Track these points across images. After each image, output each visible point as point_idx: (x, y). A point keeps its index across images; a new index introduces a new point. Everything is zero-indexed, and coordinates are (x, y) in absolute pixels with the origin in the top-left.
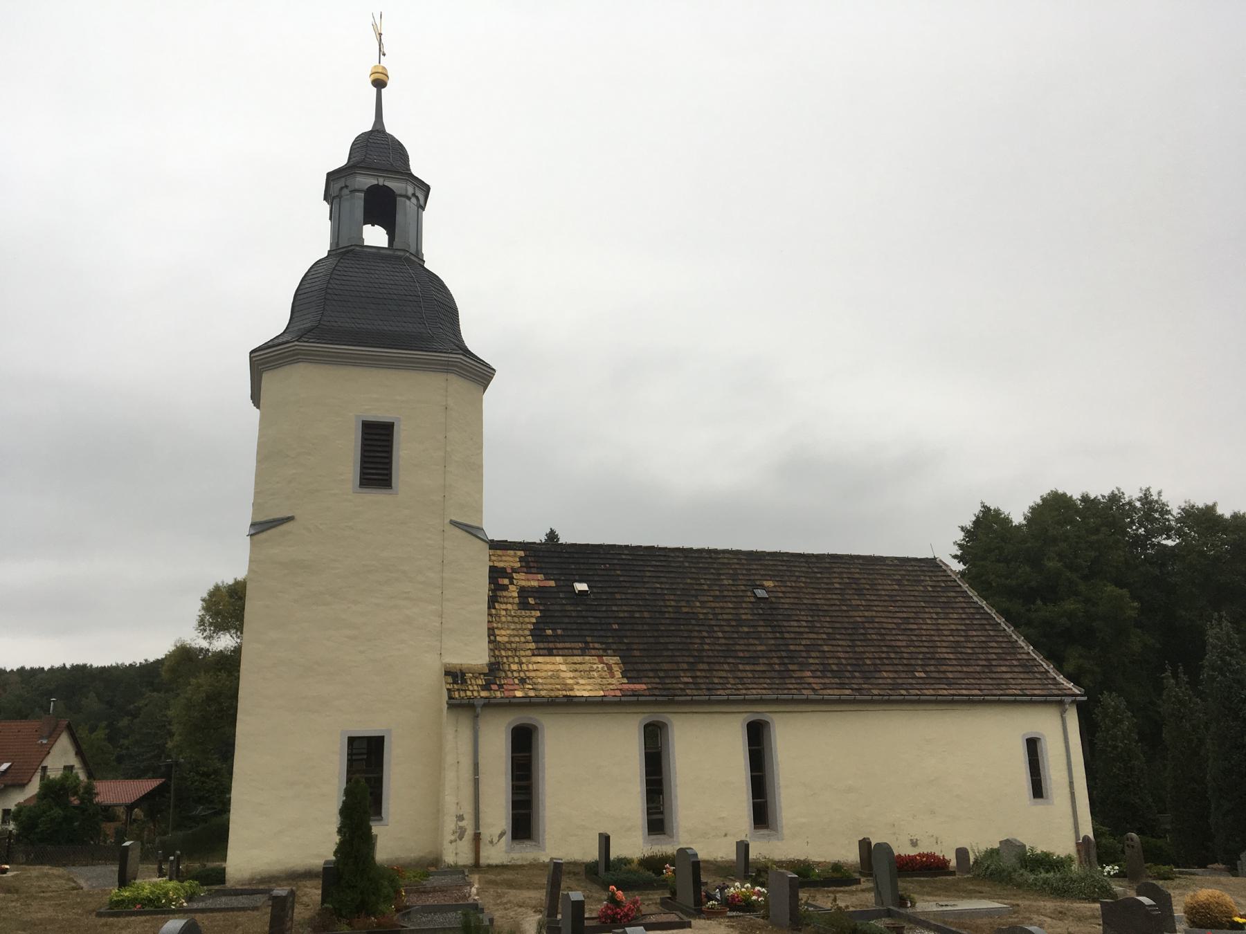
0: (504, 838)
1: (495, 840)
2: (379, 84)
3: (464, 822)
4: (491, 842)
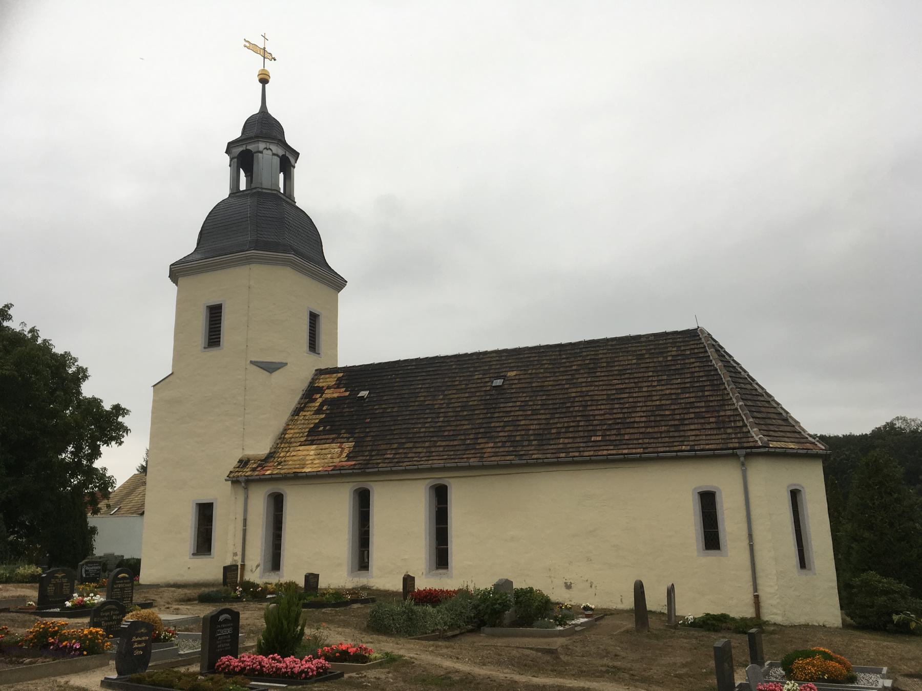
0: (259, 568)
1: (254, 569)
2: (264, 81)
3: (237, 557)
4: (252, 571)
